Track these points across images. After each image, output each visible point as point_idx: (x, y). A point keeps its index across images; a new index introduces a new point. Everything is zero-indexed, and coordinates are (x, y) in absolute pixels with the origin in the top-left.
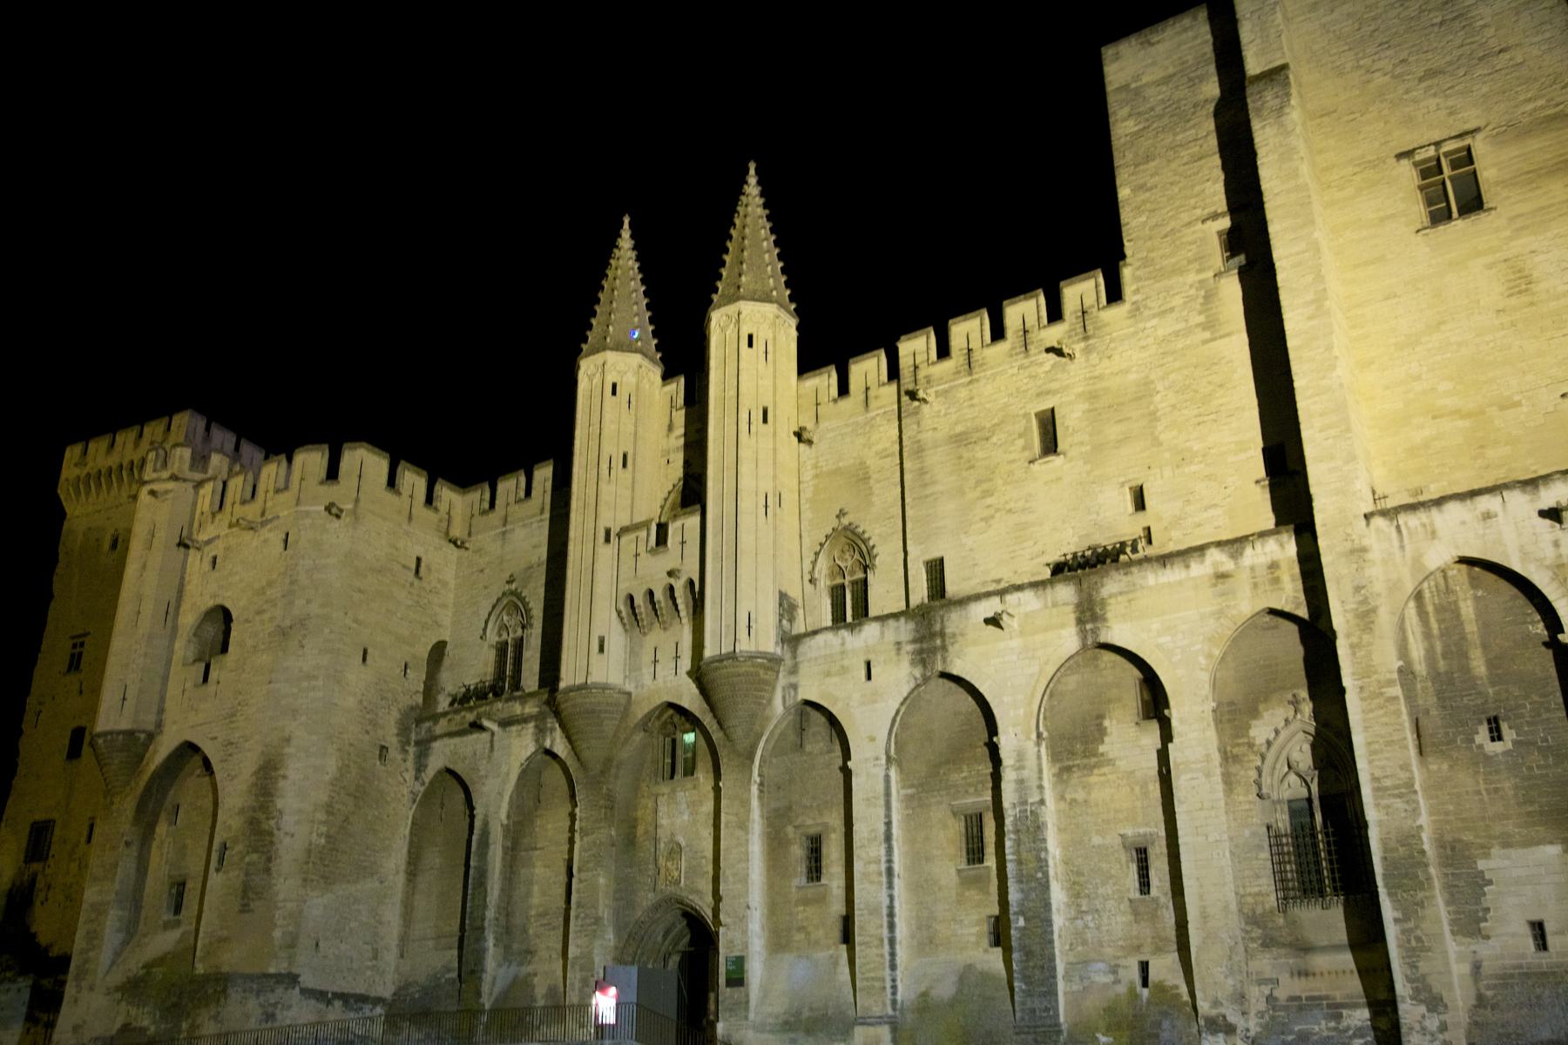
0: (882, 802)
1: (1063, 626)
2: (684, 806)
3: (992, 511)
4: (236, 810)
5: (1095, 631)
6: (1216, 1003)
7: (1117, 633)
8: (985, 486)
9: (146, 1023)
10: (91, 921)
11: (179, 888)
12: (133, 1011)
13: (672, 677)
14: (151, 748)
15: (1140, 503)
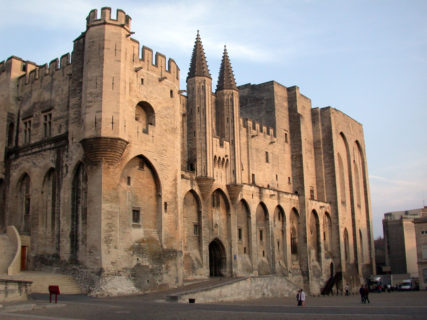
0: (255, 225)
1: (276, 200)
2: (218, 215)
3: (260, 169)
4: (169, 192)
5: (279, 202)
6: (289, 269)
7: (282, 205)
8: (260, 163)
9: (147, 264)
10: (109, 219)
11: (136, 213)
12: (140, 259)
13: (220, 182)
14: (126, 150)
15: (277, 179)
